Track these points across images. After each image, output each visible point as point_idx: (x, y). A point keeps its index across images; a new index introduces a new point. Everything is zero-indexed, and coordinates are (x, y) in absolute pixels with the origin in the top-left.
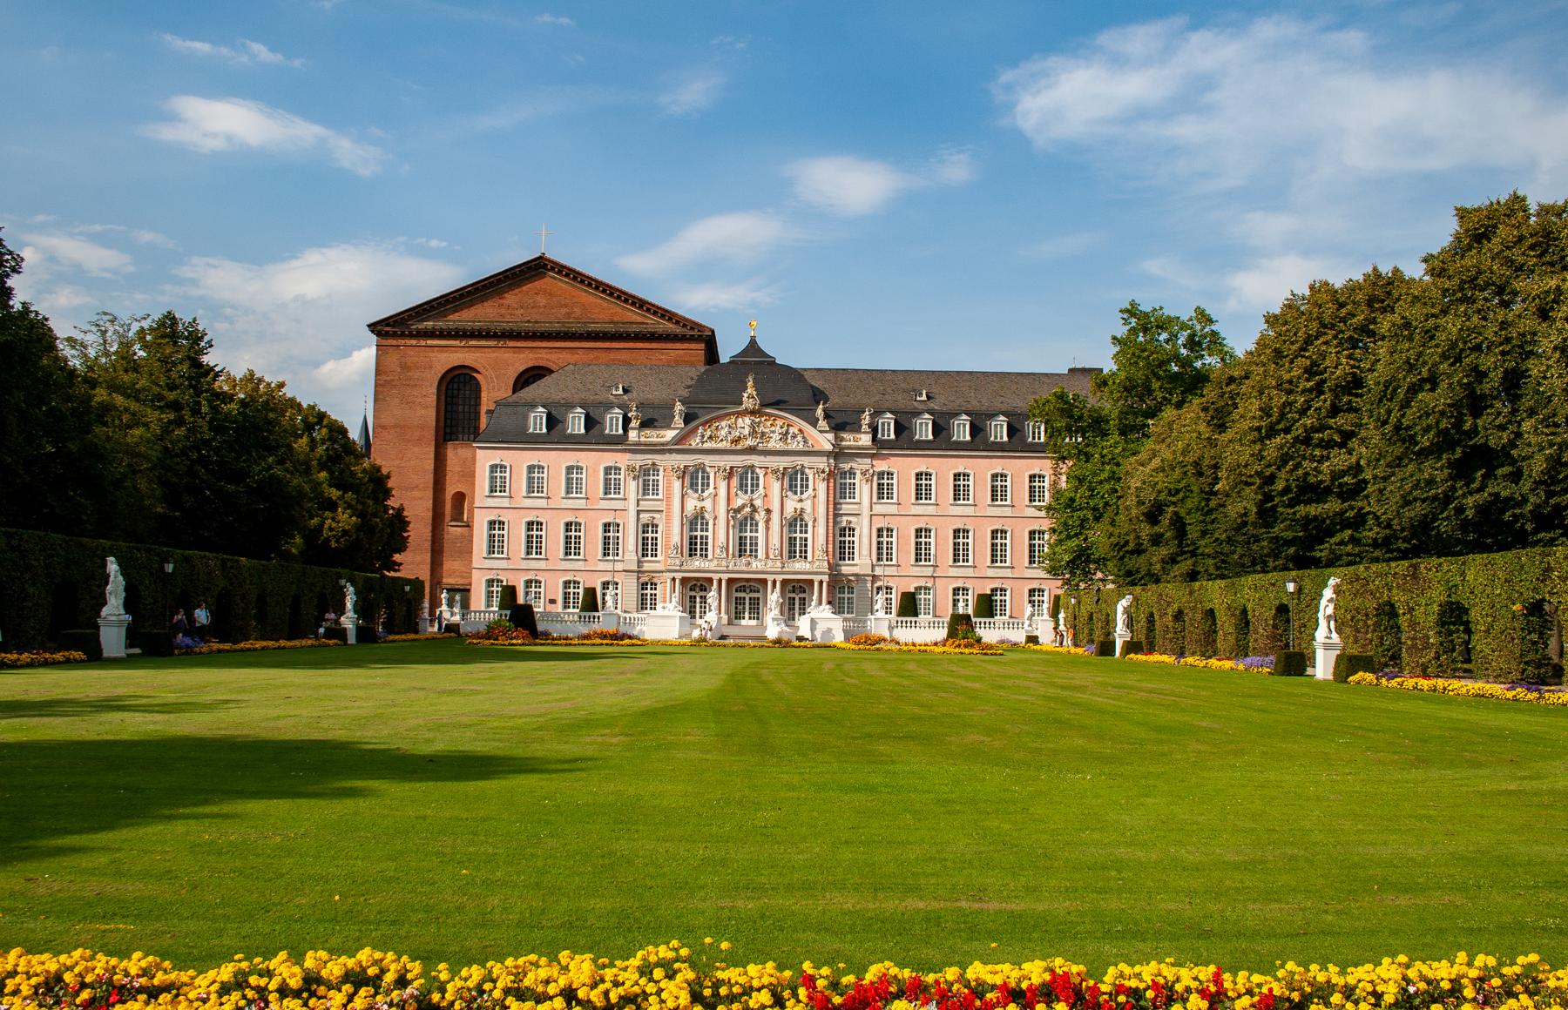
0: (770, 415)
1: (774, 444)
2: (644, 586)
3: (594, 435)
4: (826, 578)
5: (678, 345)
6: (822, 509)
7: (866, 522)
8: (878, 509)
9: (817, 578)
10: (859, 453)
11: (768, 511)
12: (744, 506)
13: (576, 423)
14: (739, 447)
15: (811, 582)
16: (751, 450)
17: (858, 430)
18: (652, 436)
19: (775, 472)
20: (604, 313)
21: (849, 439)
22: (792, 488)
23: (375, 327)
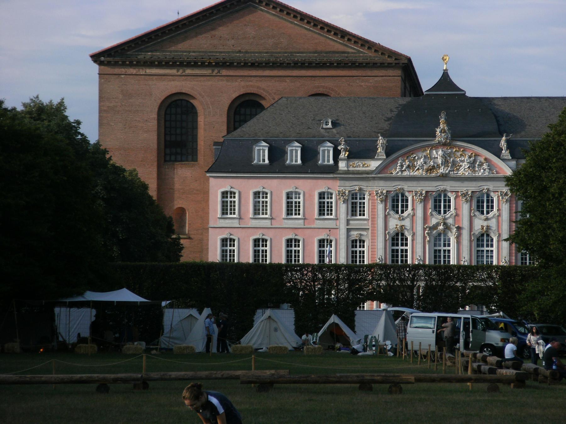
5: (376, 72)
11: (459, 229)
12: (438, 224)
13: (294, 154)
14: (433, 175)
18: (359, 165)
19: (465, 195)
22: (480, 208)
23: (96, 58)
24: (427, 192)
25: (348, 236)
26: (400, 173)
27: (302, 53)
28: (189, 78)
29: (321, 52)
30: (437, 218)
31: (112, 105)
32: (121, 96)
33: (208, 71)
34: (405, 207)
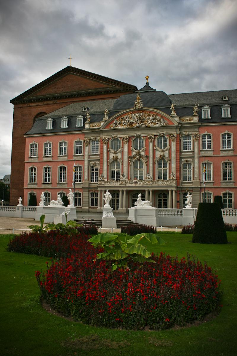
0: (147, 111)
1: (149, 125)
2: (92, 194)
3: (71, 128)
4: (174, 189)
6: (173, 155)
7: (196, 161)
8: (203, 154)
9: (170, 189)
10: (192, 126)
11: (147, 157)
12: (136, 155)
14: (132, 127)
15: (167, 191)
16: (138, 128)
17: (192, 115)
18: (95, 126)
19: (150, 137)
20: (92, 85)
21: (186, 120)
23: (12, 101)
24: (130, 137)
25: (89, 164)
26: (115, 127)
27: (90, 90)
28: (45, 106)
29: (98, 89)
30: (135, 152)
31: (17, 120)
32: (21, 116)
33: (52, 102)
34: (119, 147)
